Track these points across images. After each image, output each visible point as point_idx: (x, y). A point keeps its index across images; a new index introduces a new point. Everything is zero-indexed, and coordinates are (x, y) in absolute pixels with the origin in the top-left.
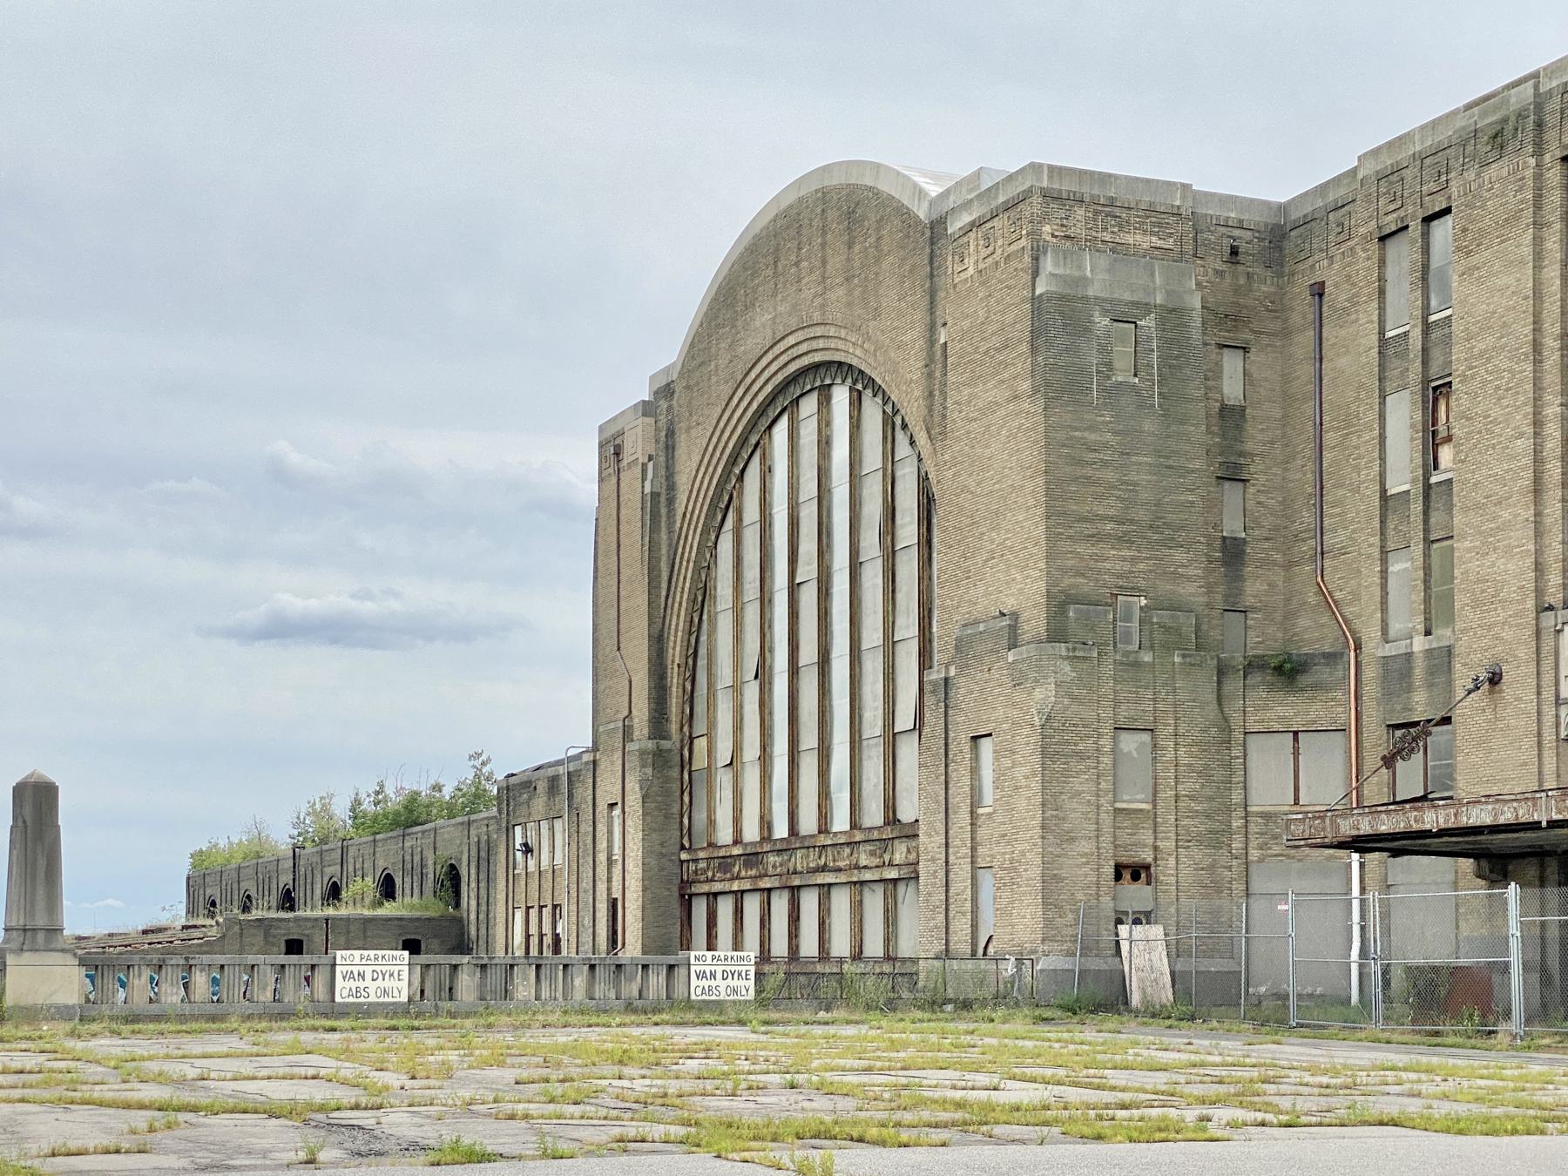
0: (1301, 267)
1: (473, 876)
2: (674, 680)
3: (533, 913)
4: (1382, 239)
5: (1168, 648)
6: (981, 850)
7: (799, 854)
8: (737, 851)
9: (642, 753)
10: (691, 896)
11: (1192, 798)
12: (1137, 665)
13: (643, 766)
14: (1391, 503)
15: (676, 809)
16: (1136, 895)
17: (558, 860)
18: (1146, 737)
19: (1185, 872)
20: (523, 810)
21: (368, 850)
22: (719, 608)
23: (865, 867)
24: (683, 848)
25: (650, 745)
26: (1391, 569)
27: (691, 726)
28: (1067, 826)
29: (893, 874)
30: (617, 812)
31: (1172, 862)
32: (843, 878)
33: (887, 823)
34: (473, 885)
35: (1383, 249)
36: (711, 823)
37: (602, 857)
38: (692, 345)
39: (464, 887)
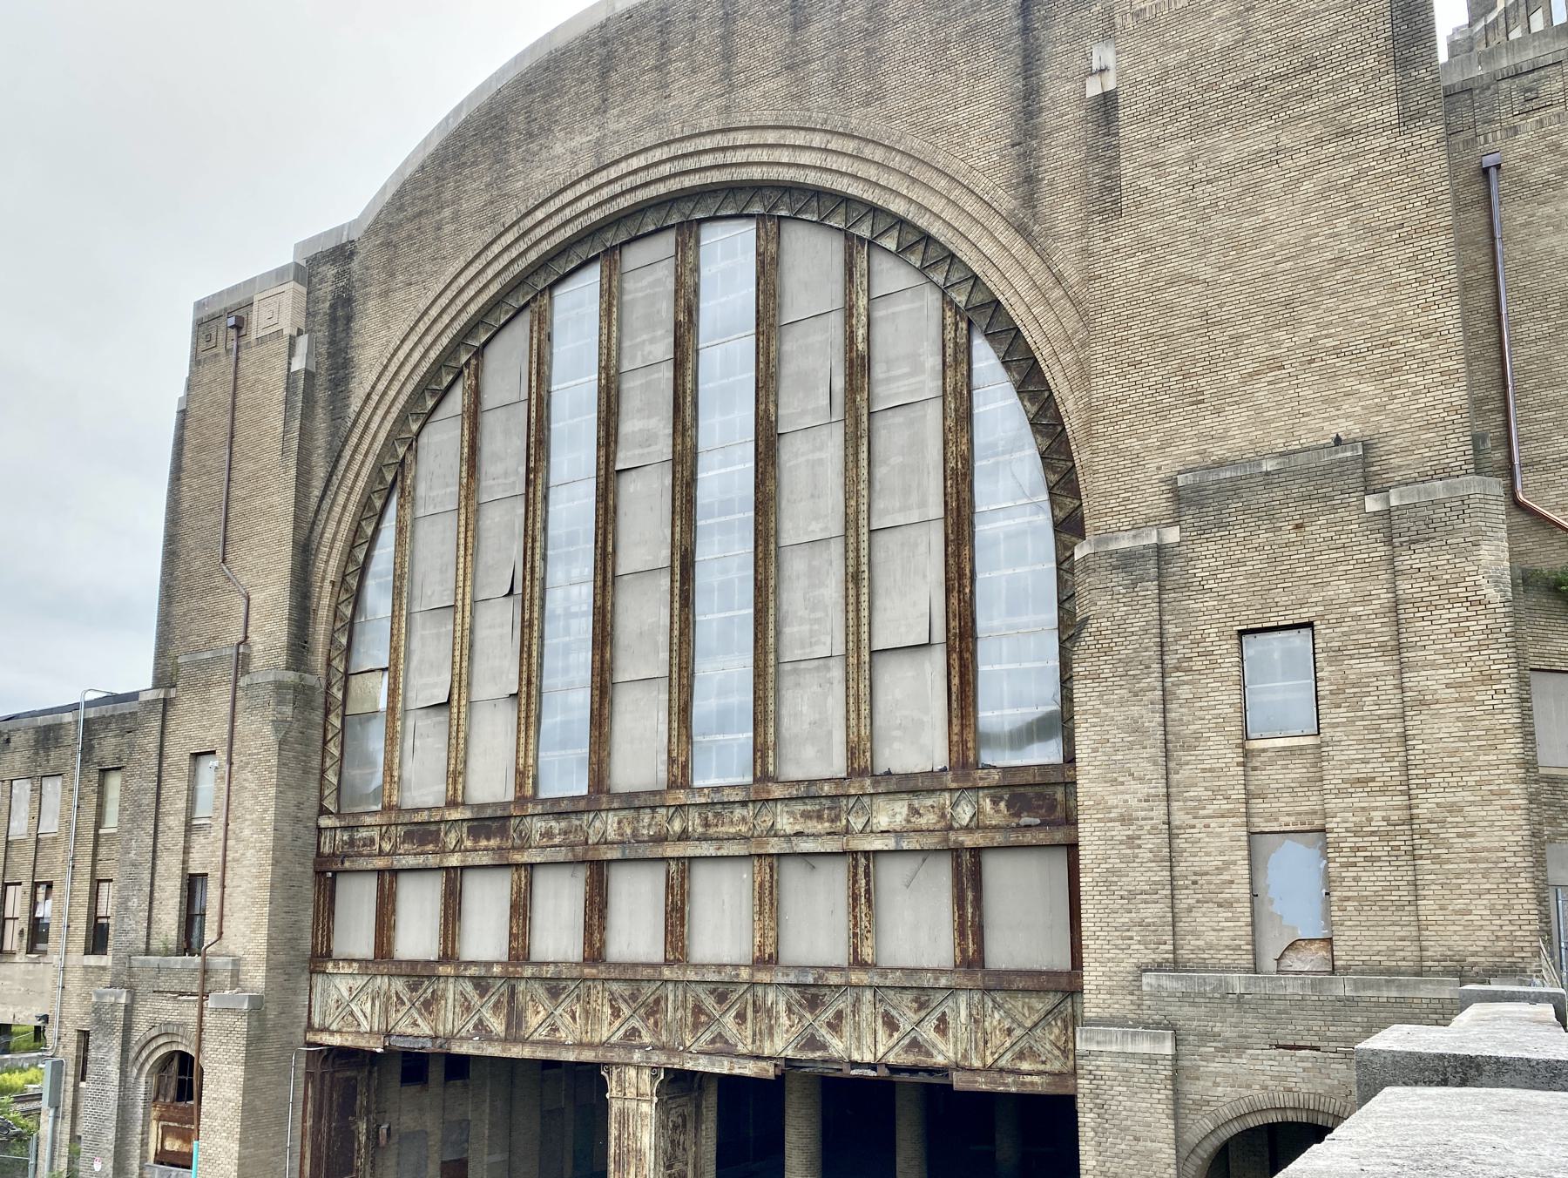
2: (324, 601)
7: (612, 820)
8: (455, 815)
9: (279, 686)
10: (335, 873)
13: (280, 702)
15: (316, 762)
22: (420, 513)
23: (798, 834)
25: (291, 677)
27: (348, 661)
29: (878, 844)
30: (208, 767)
33: (855, 772)
37: (174, 822)
38: (400, 194)
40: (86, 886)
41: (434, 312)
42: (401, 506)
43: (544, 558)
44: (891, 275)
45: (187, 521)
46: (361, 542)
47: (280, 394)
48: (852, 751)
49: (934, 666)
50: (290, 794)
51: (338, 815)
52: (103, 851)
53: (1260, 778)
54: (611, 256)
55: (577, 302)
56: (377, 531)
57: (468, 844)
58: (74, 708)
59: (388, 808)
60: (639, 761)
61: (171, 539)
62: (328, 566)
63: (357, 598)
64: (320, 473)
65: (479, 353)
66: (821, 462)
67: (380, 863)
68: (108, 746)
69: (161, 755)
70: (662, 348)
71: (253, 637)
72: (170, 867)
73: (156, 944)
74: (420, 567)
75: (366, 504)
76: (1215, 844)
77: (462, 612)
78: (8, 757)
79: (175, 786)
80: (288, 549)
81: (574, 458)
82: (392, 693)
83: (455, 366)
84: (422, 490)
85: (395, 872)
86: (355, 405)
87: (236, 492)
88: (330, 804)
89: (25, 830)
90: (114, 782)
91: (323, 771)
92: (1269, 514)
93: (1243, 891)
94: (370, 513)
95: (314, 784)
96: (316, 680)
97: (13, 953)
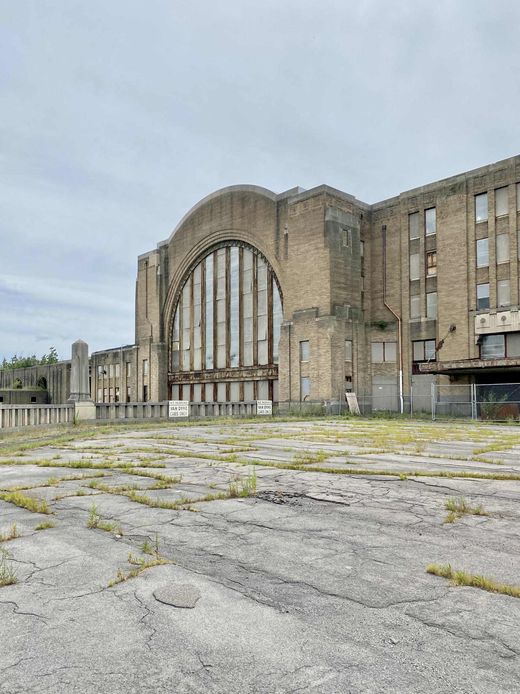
0: (377, 221)
3: (106, 391)
4: (409, 215)
5: (356, 318)
6: (302, 372)
7: (217, 374)
9: (158, 346)
11: (360, 359)
12: (349, 323)
14: (412, 283)
15: (167, 361)
16: (349, 385)
17: (118, 375)
18: (350, 342)
19: (359, 378)
20: (103, 362)
22: (184, 307)
24: (169, 372)
25: (160, 344)
26: (412, 300)
28: (336, 366)
29: (258, 379)
30: (147, 363)
31: (356, 376)
32: (236, 380)
33: (254, 365)
35: (409, 217)
36: (181, 364)
37: (140, 375)
39: (48, 384)
41: (183, 263)
42: (180, 305)
43: (205, 318)
44: (261, 263)
45: (139, 308)
46: (173, 312)
47: (155, 280)
48: (254, 361)
49: (266, 343)
50: (161, 369)
51: (172, 372)
53: (302, 368)
54: (215, 252)
55: (209, 260)
56: (176, 310)
57: (194, 379)
58: (120, 348)
59: (180, 371)
60: (221, 363)
61: (137, 312)
62: (167, 319)
63: (173, 326)
64: (164, 298)
65: (193, 272)
66: (249, 301)
67: (179, 383)
68: (128, 357)
69: (137, 360)
70: (224, 274)
71: (153, 335)
72: (140, 384)
73: (138, 400)
74: (184, 319)
75: (174, 305)
76: (296, 379)
77: (192, 329)
79: (140, 367)
80: (158, 315)
81: (210, 298)
82: (180, 346)
83: (188, 275)
84: (184, 302)
85: (182, 385)
86: (170, 283)
87: (148, 302)
88: (170, 370)
90: (129, 365)
91: (168, 363)
92: (303, 321)
93: (299, 387)
94: (175, 306)
95: (166, 366)
96: (166, 344)
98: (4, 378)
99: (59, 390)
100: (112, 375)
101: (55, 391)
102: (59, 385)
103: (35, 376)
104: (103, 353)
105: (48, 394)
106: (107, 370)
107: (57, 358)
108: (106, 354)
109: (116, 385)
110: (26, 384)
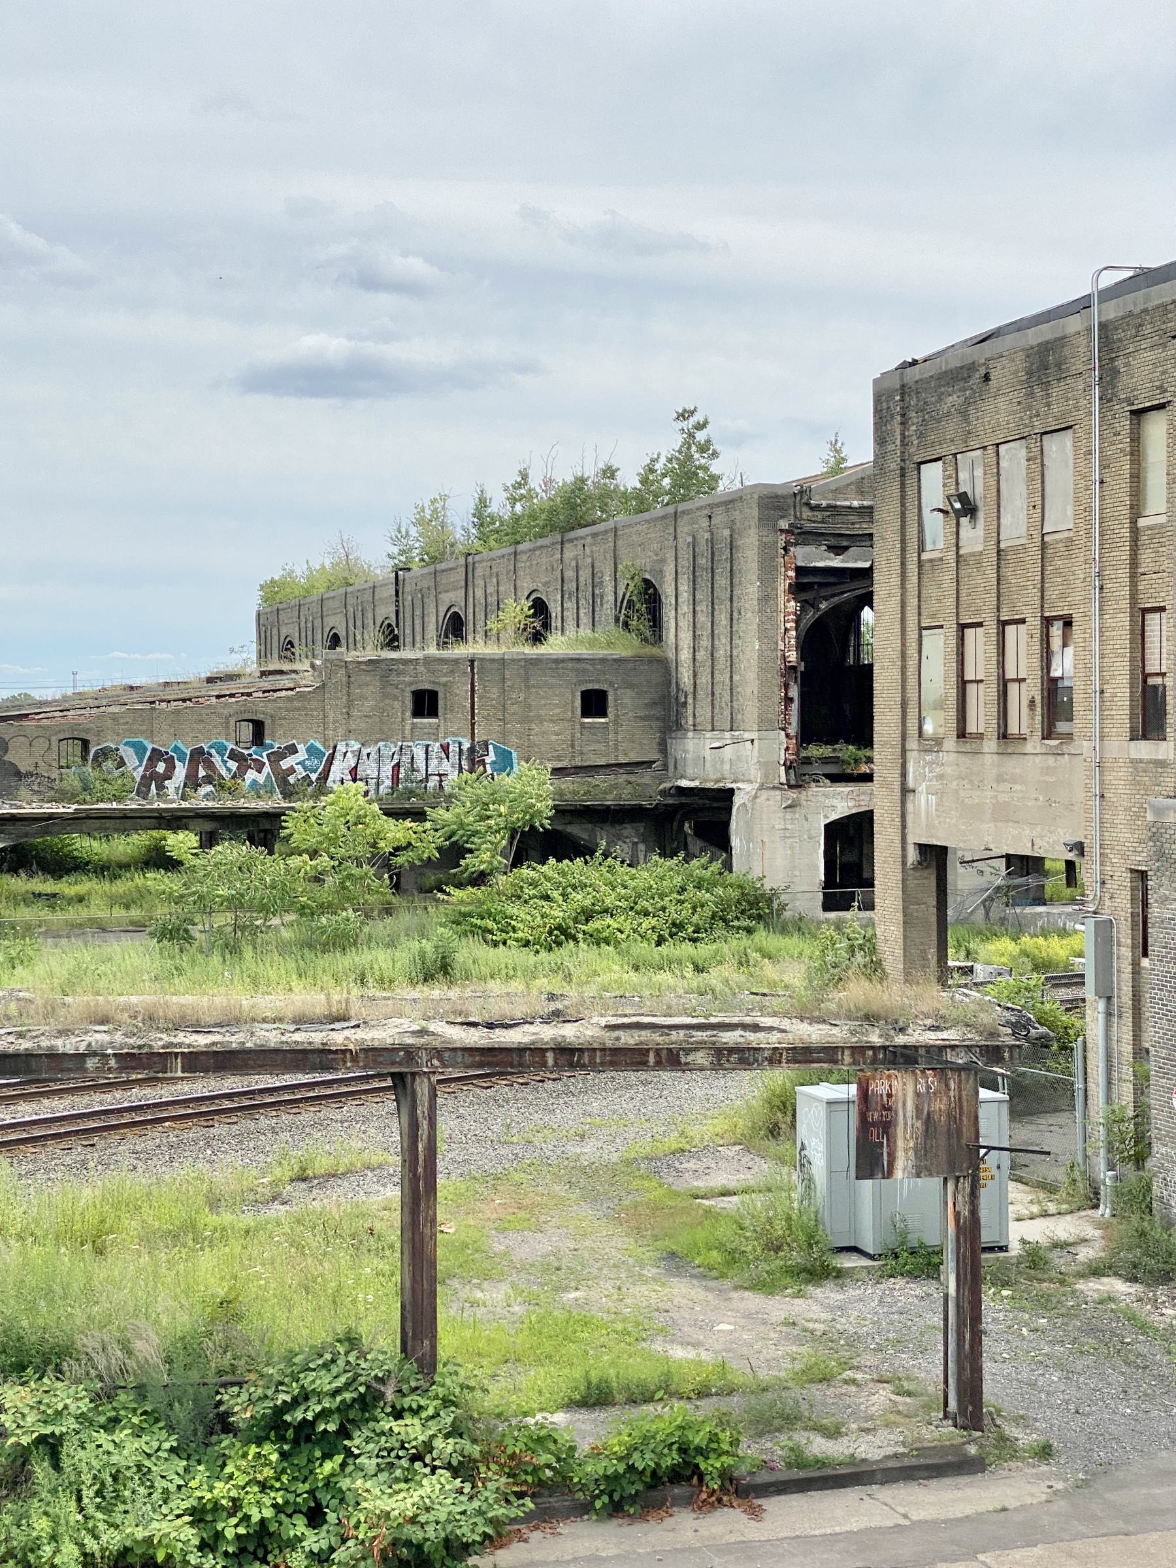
1: (685, 596)
3: (979, 644)
17: (1061, 517)
20: (950, 428)
21: (503, 567)
34: (685, 608)
39: (668, 615)
40: (1124, 621)
52: (1146, 557)
58: (1084, 304)
78: (988, 406)
89: (1023, 531)
97: (1022, 739)
98: (479, 593)
99: (722, 653)
100: (1016, 525)
101: (700, 656)
102: (723, 619)
103: (607, 578)
104: (955, 363)
105: (668, 671)
106: (979, 491)
107: (715, 468)
108: (972, 367)
109: (1051, 594)
110: (570, 615)
